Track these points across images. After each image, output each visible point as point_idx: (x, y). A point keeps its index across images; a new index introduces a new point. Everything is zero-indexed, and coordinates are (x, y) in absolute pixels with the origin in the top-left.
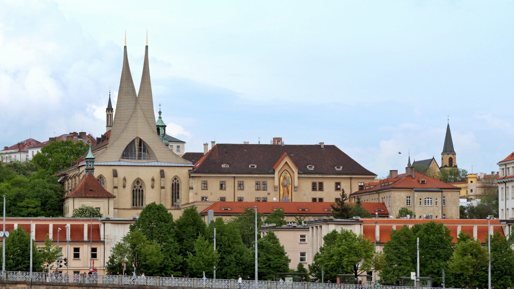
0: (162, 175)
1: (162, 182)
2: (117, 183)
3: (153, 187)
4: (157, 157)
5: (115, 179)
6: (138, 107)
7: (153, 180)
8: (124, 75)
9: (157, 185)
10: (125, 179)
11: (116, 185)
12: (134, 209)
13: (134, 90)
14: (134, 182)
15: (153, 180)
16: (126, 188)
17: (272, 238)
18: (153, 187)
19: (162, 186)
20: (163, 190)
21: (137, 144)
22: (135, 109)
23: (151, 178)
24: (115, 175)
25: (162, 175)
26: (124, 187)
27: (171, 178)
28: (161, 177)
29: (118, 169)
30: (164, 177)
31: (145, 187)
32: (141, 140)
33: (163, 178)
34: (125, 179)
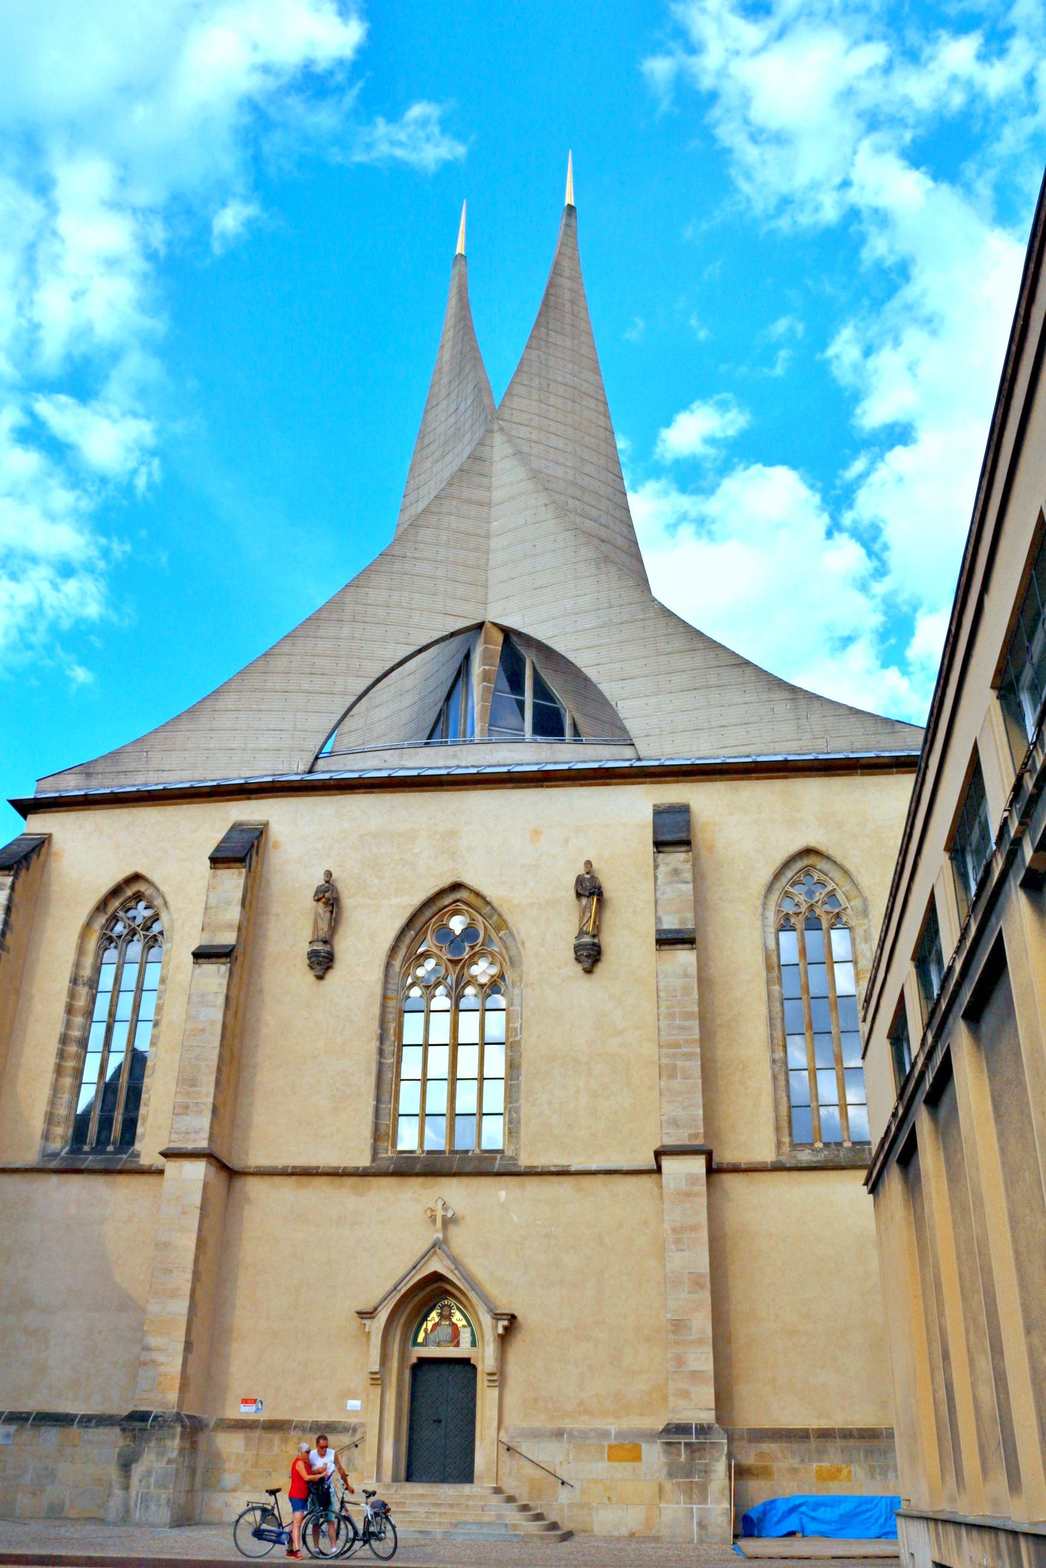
0: (673, 834)
3: (590, 955)
4: (633, 726)
5: (233, 880)
6: (499, 449)
7: (590, 890)
8: (446, 369)
9: (628, 936)
10: (329, 897)
11: (228, 938)
15: (590, 890)
18: (590, 955)
19: (670, 923)
20: (685, 957)
22: (475, 465)
24: (241, 852)
25: (673, 834)
26: (322, 962)
28: (660, 845)
32: (514, 648)
33: (677, 858)
34: (329, 897)
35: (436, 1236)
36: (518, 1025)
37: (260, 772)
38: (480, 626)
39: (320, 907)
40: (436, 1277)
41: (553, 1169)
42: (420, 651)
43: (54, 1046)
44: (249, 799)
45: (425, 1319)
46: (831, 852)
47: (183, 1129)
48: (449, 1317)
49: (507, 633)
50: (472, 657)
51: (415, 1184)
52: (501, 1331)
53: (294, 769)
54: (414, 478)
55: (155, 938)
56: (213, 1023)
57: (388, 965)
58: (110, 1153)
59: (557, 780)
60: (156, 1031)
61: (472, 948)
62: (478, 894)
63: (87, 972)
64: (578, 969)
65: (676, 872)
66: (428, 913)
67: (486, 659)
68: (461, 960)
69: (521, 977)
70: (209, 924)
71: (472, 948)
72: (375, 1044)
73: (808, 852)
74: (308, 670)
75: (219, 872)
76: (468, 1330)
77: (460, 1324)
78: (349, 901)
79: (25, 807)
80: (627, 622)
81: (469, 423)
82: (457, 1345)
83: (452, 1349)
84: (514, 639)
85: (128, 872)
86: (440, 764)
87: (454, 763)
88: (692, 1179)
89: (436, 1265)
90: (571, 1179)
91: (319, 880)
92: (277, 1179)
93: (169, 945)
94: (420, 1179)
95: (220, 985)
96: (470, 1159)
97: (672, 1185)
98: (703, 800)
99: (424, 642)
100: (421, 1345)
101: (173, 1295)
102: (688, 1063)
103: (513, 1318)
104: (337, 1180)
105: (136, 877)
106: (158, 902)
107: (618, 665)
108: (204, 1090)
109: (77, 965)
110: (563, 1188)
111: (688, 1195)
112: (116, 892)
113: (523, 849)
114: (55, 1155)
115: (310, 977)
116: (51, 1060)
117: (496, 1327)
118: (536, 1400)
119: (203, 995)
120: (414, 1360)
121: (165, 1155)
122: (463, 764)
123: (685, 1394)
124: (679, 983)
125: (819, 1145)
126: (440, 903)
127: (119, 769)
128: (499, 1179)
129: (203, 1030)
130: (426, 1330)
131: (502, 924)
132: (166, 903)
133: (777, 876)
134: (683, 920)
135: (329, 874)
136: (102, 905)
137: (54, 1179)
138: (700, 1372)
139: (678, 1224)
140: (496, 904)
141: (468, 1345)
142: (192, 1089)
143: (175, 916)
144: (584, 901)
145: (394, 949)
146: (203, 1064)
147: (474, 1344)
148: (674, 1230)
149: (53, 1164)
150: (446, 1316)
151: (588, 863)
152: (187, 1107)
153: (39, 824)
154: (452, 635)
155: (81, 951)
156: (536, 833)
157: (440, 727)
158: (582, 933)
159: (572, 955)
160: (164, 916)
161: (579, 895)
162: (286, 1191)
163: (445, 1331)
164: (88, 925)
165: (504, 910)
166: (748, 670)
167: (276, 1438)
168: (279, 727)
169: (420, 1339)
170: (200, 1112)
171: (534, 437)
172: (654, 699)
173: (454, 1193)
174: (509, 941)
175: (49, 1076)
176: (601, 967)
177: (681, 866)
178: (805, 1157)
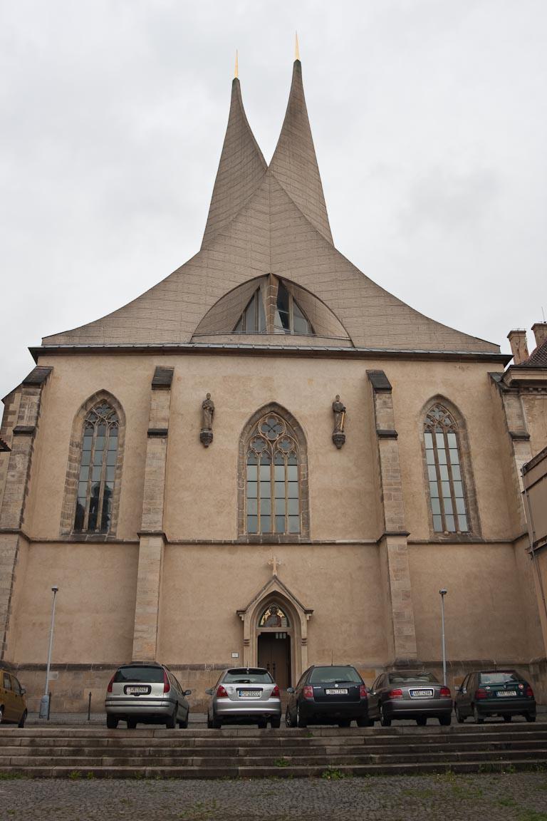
0: (380, 385)
1: (382, 413)
2: (165, 413)
3: (338, 441)
10: (208, 408)
11: (162, 425)
12: (254, 543)
13: (257, 153)
14: (252, 422)
16: (214, 446)
17: (433, 680)
19: (383, 427)
20: (391, 443)
21: (268, 296)
23: (328, 404)
25: (380, 385)
26: (206, 439)
27: (419, 405)
29: (182, 368)
30: (389, 389)
31: (304, 442)
33: (385, 396)
34: (208, 408)
35: (274, 574)
36: (305, 473)
37: (167, 340)
38: (268, 275)
39: (207, 413)
40: (275, 593)
41: (327, 542)
42: (240, 286)
43: (64, 478)
44: (164, 355)
45: (264, 614)
46: (452, 399)
47: (148, 521)
48: (276, 612)
49: (280, 279)
50: (262, 290)
51: (260, 548)
52: (308, 619)
53: (183, 340)
54: (216, 195)
55: (114, 424)
56: (160, 468)
57: (240, 441)
58: (97, 533)
59: (317, 355)
60: (118, 472)
61: (280, 435)
62: (283, 409)
63: (78, 440)
64: (333, 447)
65: (385, 403)
66: (258, 416)
67: (270, 293)
68: (275, 441)
69: (306, 450)
70: (153, 418)
71: (280, 435)
72: (236, 481)
73: (439, 397)
74: (186, 291)
75: (157, 392)
76: (285, 619)
77: (281, 616)
78: (218, 410)
79: (36, 353)
80: (345, 280)
81: (251, 171)
82: (280, 626)
83: (277, 628)
84: (283, 282)
85: (100, 389)
86: (260, 344)
87: (267, 343)
88: (401, 547)
89: (275, 588)
90: (336, 547)
91: (203, 396)
92: (189, 547)
93: (122, 428)
94: (262, 547)
95: (163, 449)
96: (285, 536)
97: (392, 550)
98: (392, 371)
99: (243, 281)
100: (262, 626)
101: (149, 604)
102: (396, 493)
103: (311, 612)
104: (221, 547)
105: (104, 392)
106: (114, 405)
107: (342, 301)
108: (158, 502)
109: (72, 436)
110: (332, 551)
111: (400, 554)
112: (92, 399)
113: (309, 390)
114: (67, 534)
115: (200, 447)
116: (63, 485)
117: (306, 617)
118: (323, 651)
119: (154, 454)
120: (260, 634)
121: (140, 535)
122: (272, 344)
123: (403, 647)
124: (390, 455)
125: (446, 533)
126: (263, 412)
127: (88, 335)
128: (302, 547)
129: (155, 471)
130: (264, 619)
131: (296, 423)
132: (120, 407)
133: (424, 407)
134: (389, 426)
135: (208, 395)
136: (84, 406)
137: (69, 547)
138: (410, 636)
139: (396, 568)
140: (293, 414)
141: (286, 626)
142: (151, 501)
143: (126, 413)
144: (338, 415)
145: (242, 434)
146: (157, 489)
147: (288, 625)
148: (394, 571)
149: (69, 539)
150: (274, 612)
151: (338, 397)
152: (150, 510)
153: (45, 362)
154: (255, 279)
155: (74, 429)
156: (311, 380)
157: (239, 326)
158: (335, 430)
159: (330, 440)
160: (119, 413)
161: (334, 411)
162: (195, 553)
163: (274, 620)
164: (77, 416)
165: (297, 417)
166: (406, 308)
167: (198, 673)
168: (173, 319)
169: (262, 624)
170: (157, 513)
171: (288, 181)
172: (360, 319)
173: (279, 556)
174: (298, 433)
175: (62, 493)
176: (346, 446)
177: (387, 400)
178: (441, 538)
